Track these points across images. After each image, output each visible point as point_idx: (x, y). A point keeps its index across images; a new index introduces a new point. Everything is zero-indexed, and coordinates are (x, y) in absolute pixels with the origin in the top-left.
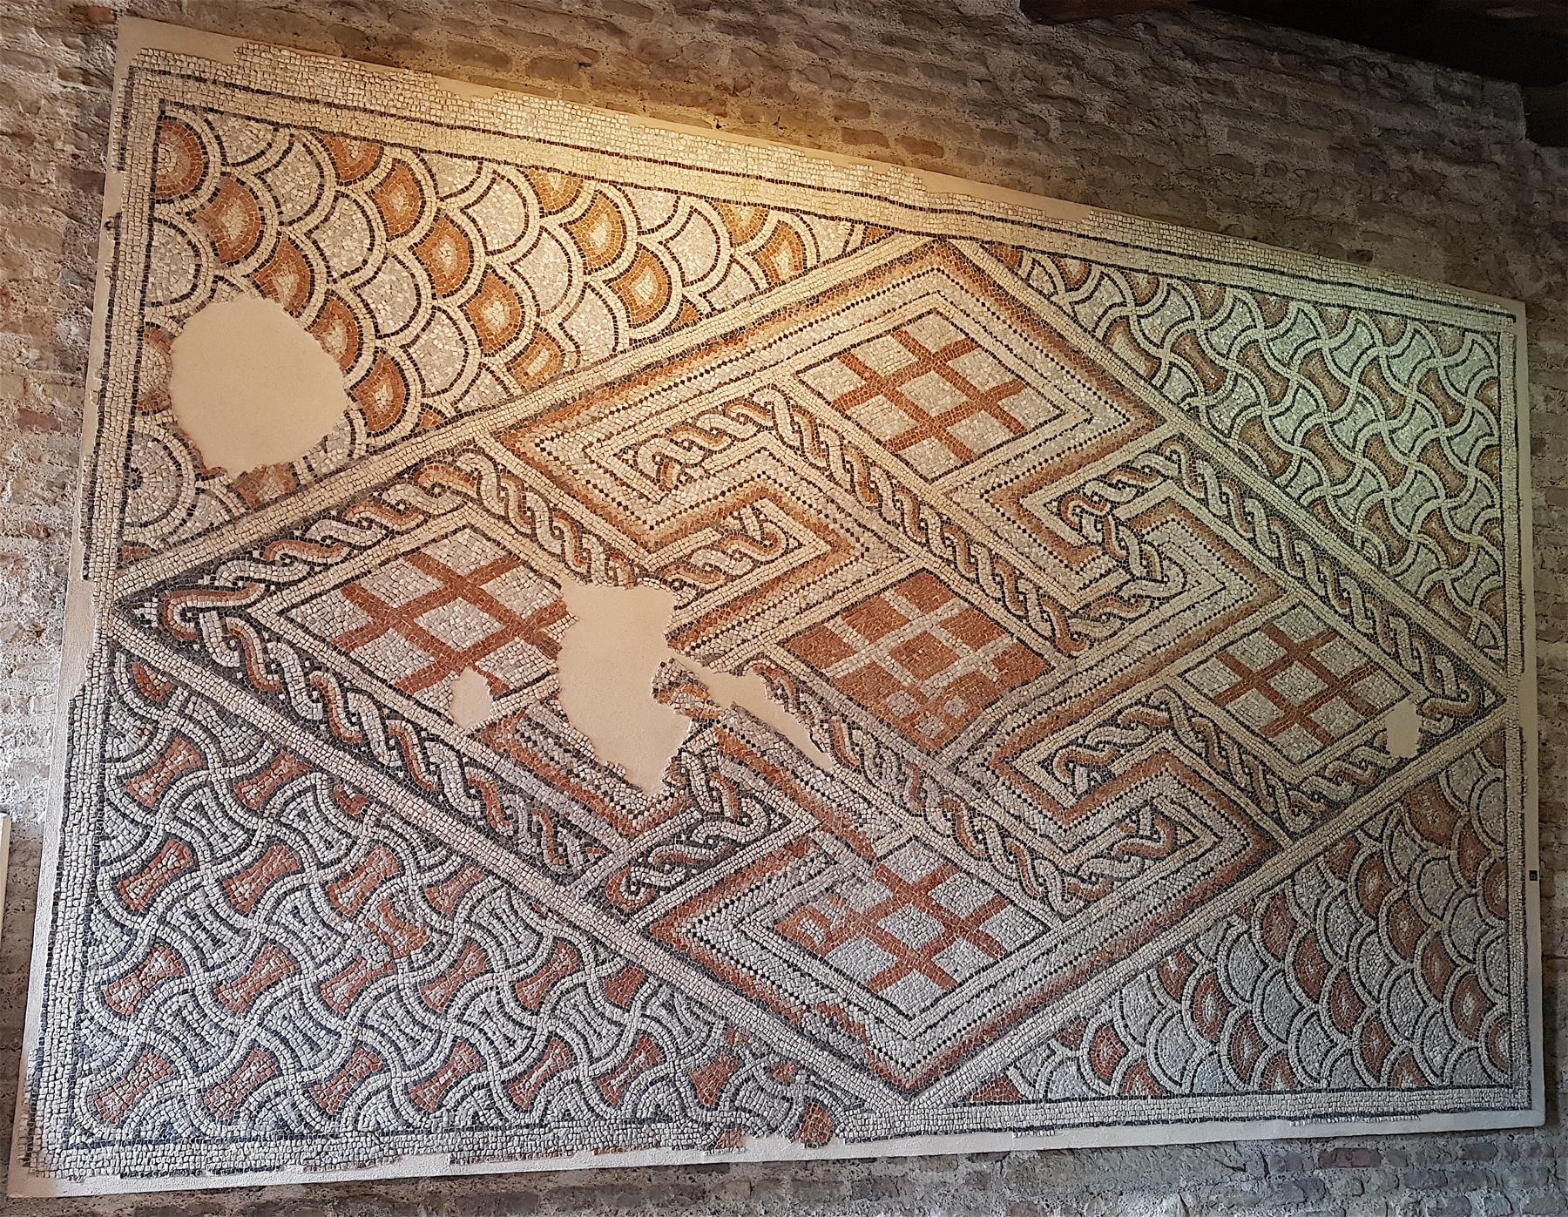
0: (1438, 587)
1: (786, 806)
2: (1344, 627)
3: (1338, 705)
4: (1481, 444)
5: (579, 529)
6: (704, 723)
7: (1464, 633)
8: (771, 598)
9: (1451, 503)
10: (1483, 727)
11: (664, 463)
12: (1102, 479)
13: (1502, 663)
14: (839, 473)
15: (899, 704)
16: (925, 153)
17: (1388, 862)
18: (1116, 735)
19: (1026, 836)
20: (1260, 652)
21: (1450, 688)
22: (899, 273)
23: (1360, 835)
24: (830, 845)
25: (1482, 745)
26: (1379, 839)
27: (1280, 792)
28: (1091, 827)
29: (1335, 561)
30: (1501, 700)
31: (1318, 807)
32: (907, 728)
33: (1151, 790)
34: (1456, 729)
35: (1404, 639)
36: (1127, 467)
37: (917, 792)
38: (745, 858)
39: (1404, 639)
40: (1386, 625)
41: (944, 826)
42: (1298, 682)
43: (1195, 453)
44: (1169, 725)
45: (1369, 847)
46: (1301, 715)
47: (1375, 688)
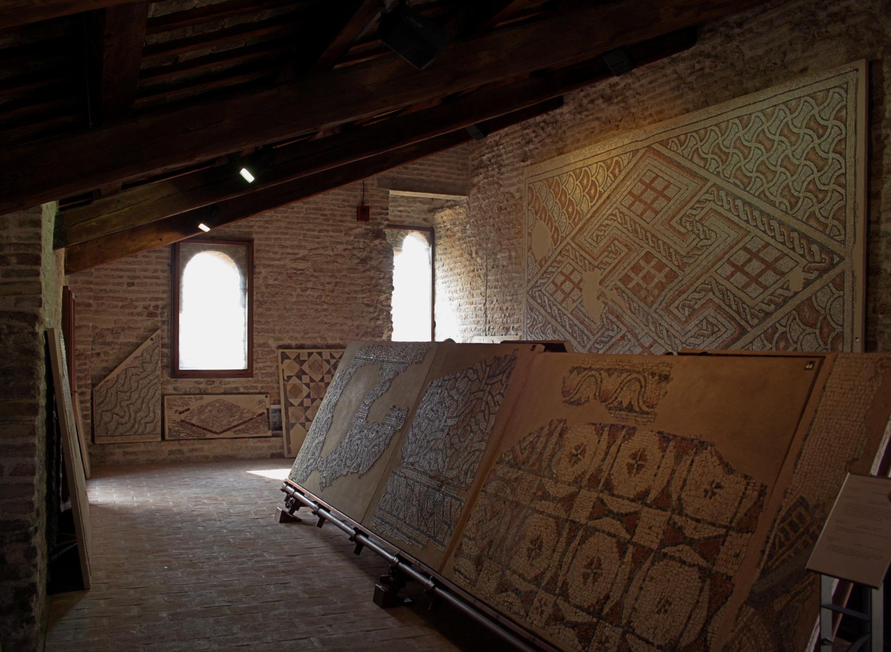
0: (813, 214)
1: (621, 326)
2: (772, 241)
3: (770, 273)
4: (836, 140)
5: (585, 259)
6: (606, 304)
7: (823, 232)
8: (617, 268)
9: (819, 174)
10: (833, 273)
11: (598, 236)
12: (692, 208)
13: (843, 242)
14: (630, 228)
15: (643, 293)
16: (660, 116)
17: (788, 335)
18: (696, 296)
19: (673, 331)
20: (742, 257)
21: (817, 258)
22: (641, 163)
23: (777, 325)
24: (629, 336)
25: (833, 281)
26: (785, 327)
27: (747, 310)
28: (689, 328)
29: (768, 215)
30: (842, 259)
31: (761, 315)
32: (644, 300)
33: (706, 314)
34: (820, 276)
35: (796, 242)
36: (698, 202)
37: (647, 319)
38: (614, 340)
39: (796, 242)
40: (789, 236)
41: (653, 329)
42: (755, 267)
43: (720, 189)
44: (711, 290)
45: (781, 329)
46: (755, 279)
47: (783, 265)
